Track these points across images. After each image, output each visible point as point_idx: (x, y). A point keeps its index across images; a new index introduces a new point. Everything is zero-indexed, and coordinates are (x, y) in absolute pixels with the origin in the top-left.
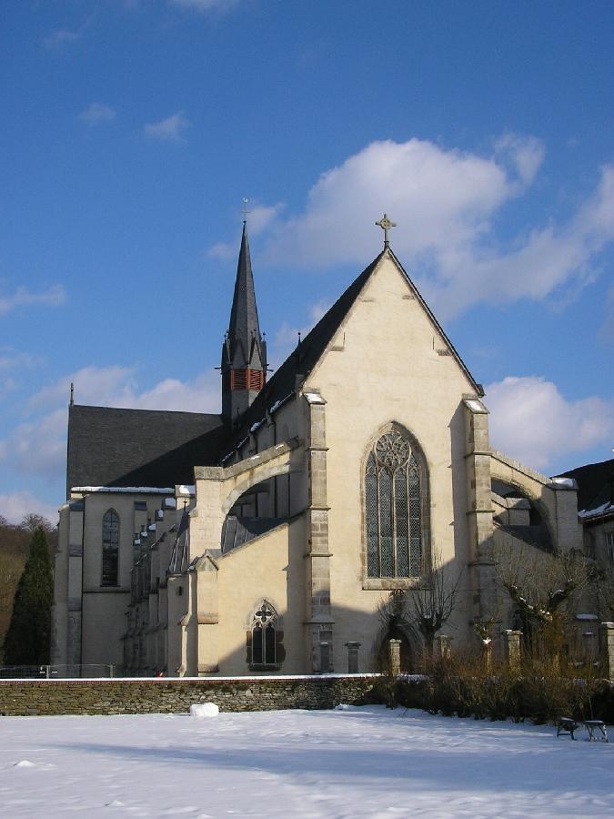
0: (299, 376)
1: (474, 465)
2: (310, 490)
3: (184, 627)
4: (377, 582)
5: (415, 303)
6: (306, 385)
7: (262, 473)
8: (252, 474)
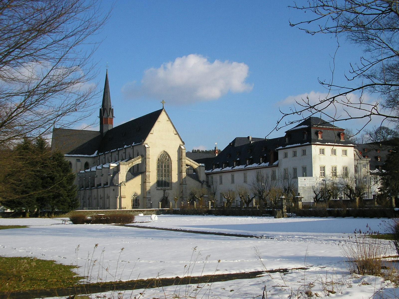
0: (143, 140)
1: (182, 161)
2: (146, 168)
3: (118, 199)
4: (160, 188)
5: (169, 122)
6: (146, 142)
7: (134, 163)
8: (132, 164)
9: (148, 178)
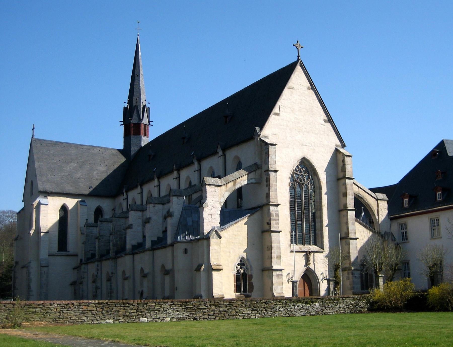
1: (345, 184)
4: (298, 247)
7: (240, 183)
9: (274, 220)
